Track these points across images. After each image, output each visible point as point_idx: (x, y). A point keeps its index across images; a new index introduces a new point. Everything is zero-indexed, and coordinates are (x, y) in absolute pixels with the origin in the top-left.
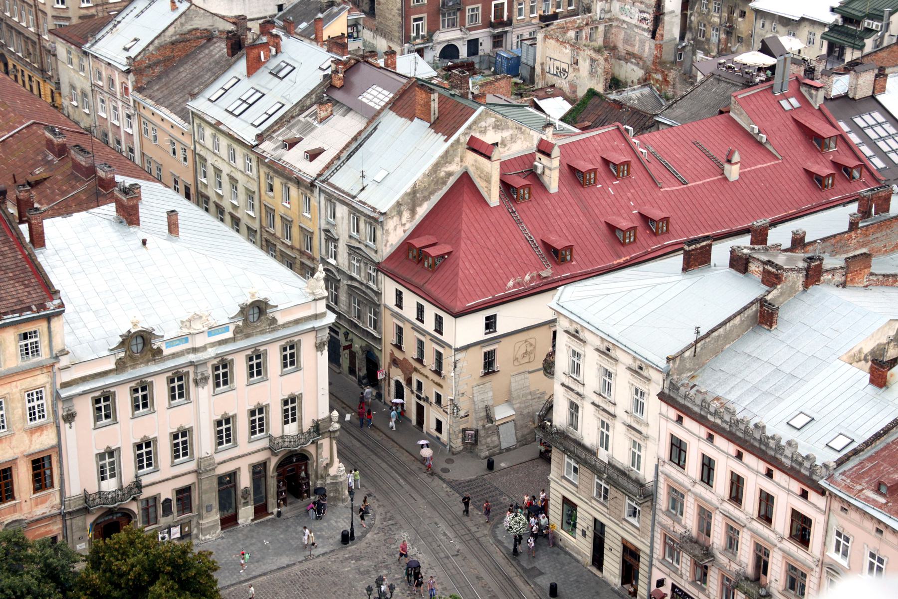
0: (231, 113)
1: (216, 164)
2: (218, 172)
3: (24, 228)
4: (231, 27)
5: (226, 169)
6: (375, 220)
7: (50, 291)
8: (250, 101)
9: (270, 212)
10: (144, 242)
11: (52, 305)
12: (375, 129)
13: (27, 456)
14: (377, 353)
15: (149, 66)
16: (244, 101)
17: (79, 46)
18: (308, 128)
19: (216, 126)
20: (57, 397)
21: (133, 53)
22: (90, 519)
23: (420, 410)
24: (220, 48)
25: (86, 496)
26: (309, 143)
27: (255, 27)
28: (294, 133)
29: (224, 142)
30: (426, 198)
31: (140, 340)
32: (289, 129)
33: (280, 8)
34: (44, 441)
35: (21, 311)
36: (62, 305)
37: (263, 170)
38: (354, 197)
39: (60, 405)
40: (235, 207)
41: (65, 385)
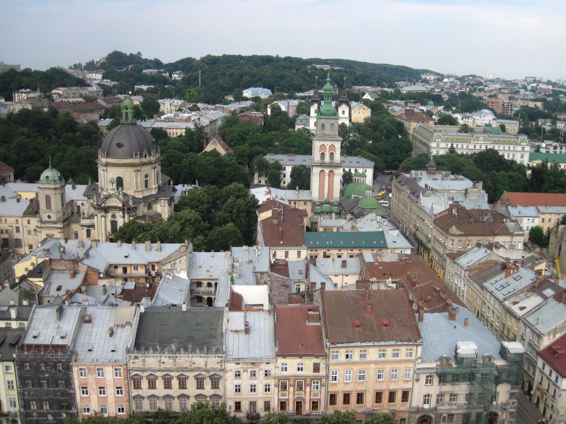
0: (497, 289)
1: (489, 306)
2: (489, 308)
3: (417, 315)
4: (505, 261)
5: (492, 308)
6: (539, 336)
7: (419, 337)
8: (504, 286)
9: (504, 326)
10: (455, 327)
11: (419, 342)
12: (546, 303)
13: (402, 389)
14: (532, 384)
15: (474, 270)
16: (502, 286)
17: (453, 260)
18: (523, 299)
19: (491, 293)
20: (415, 372)
21: (469, 265)
22: (418, 416)
23: (545, 409)
24: (499, 267)
25: (418, 408)
26: (521, 304)
27: (512, 261)
28: (517, 300)
29: (493, 298)
30: (560, 332)
31: (446, 360)
32: (516, 298)
33: (523, 257)
34: (408, 386)
35: (409, 341)
36: (422, 342)
37: (504, 311)
38: (533, 326)
39: (415, 375)
40: (492, 321)
41: (418, 369)
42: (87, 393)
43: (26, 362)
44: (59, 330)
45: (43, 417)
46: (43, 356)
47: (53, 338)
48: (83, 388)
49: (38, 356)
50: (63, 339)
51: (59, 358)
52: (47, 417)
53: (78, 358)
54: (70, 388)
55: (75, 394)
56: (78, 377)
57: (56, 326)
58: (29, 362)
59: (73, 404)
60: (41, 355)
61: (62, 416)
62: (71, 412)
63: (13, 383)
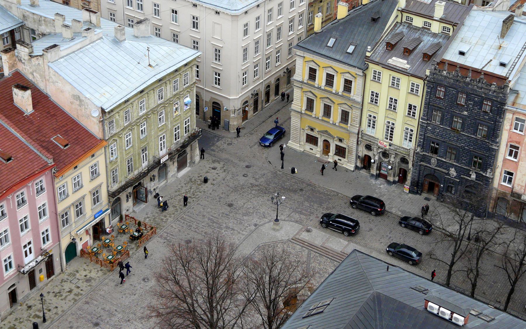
42: (515, 157)
43: (441, 85)
44: (500, 51)
45: (444, 169)
46: (468, 84)
47: (489, 63)
48: (511, 146)
49: (460, 82)
50: (502, 67)
51: (490, 93)
52: (449, 170)
53: (519, 101)
54: (493, 141)
55: (497, 151)
56: (510, 129)
57: (497, 44)
58: (445, 87)
59: (490, 165)
60: (464, 82)
61: (470, 176)
62: (484, 174)
63: (415, 110)
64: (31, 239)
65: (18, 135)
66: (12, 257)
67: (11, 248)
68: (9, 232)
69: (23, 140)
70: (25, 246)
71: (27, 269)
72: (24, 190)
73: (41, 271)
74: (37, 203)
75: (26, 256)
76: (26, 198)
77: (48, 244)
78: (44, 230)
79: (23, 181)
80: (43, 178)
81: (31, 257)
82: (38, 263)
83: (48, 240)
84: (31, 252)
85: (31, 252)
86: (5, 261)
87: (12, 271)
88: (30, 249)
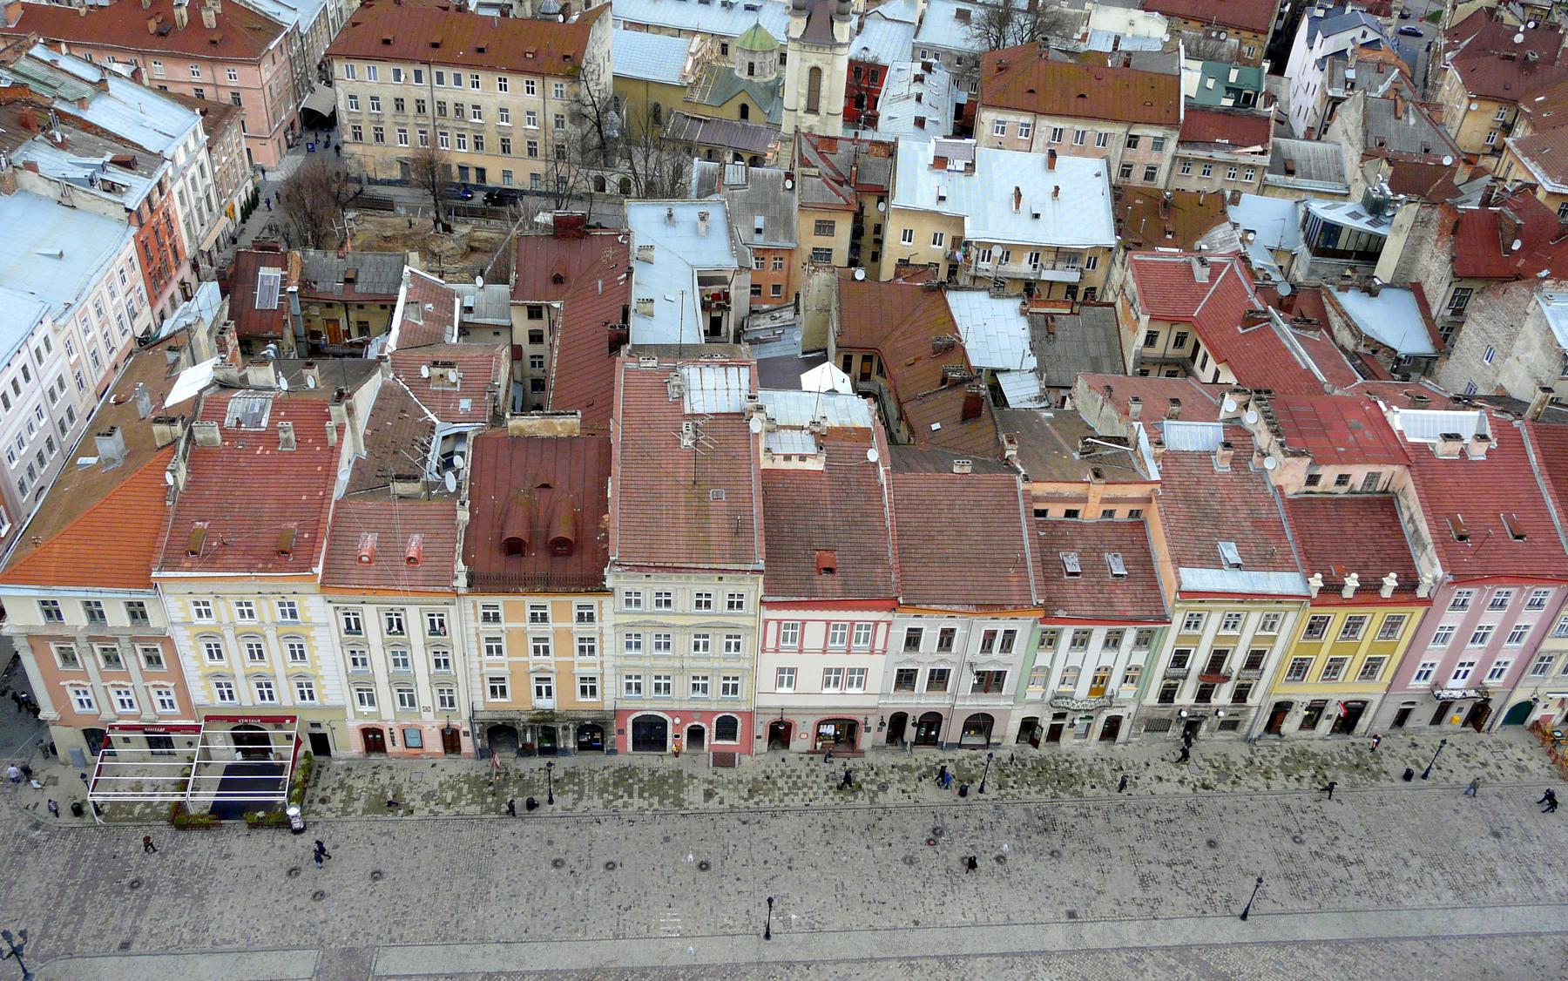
64: (1477, 661)
65: (1554, 512)
66: (1436, 667)
67: (1443, 654)
68: (1454, 632)
69: (1557, 522)
70: (1462, 665)
71: (1445, 694)
72: (1514, 591)
73: (1460, 710)
74: (1520, 618)
75: (1455, 677)
76: (1508, 603)
77: (1495, 682)
78: (1503, 660)
79: (1521, 578)
80: (1552, 591)
81: (1461, 683)
82: (1465, 697)
83: (1498, 676)
84: (1464, 677)
85: (1464, 677)
86: (1424, 665)
87: (1423, 684)
88: (1467, 672)
